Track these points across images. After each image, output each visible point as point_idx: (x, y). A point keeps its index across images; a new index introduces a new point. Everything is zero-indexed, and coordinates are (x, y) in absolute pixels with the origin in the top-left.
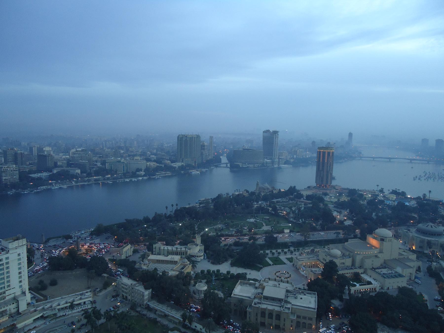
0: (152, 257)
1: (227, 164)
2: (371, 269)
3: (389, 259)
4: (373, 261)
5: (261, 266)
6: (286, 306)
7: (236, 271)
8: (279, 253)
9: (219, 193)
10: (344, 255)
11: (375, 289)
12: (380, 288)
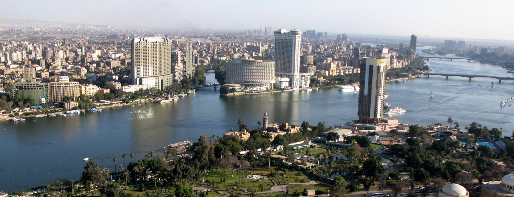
1: (215, 86)
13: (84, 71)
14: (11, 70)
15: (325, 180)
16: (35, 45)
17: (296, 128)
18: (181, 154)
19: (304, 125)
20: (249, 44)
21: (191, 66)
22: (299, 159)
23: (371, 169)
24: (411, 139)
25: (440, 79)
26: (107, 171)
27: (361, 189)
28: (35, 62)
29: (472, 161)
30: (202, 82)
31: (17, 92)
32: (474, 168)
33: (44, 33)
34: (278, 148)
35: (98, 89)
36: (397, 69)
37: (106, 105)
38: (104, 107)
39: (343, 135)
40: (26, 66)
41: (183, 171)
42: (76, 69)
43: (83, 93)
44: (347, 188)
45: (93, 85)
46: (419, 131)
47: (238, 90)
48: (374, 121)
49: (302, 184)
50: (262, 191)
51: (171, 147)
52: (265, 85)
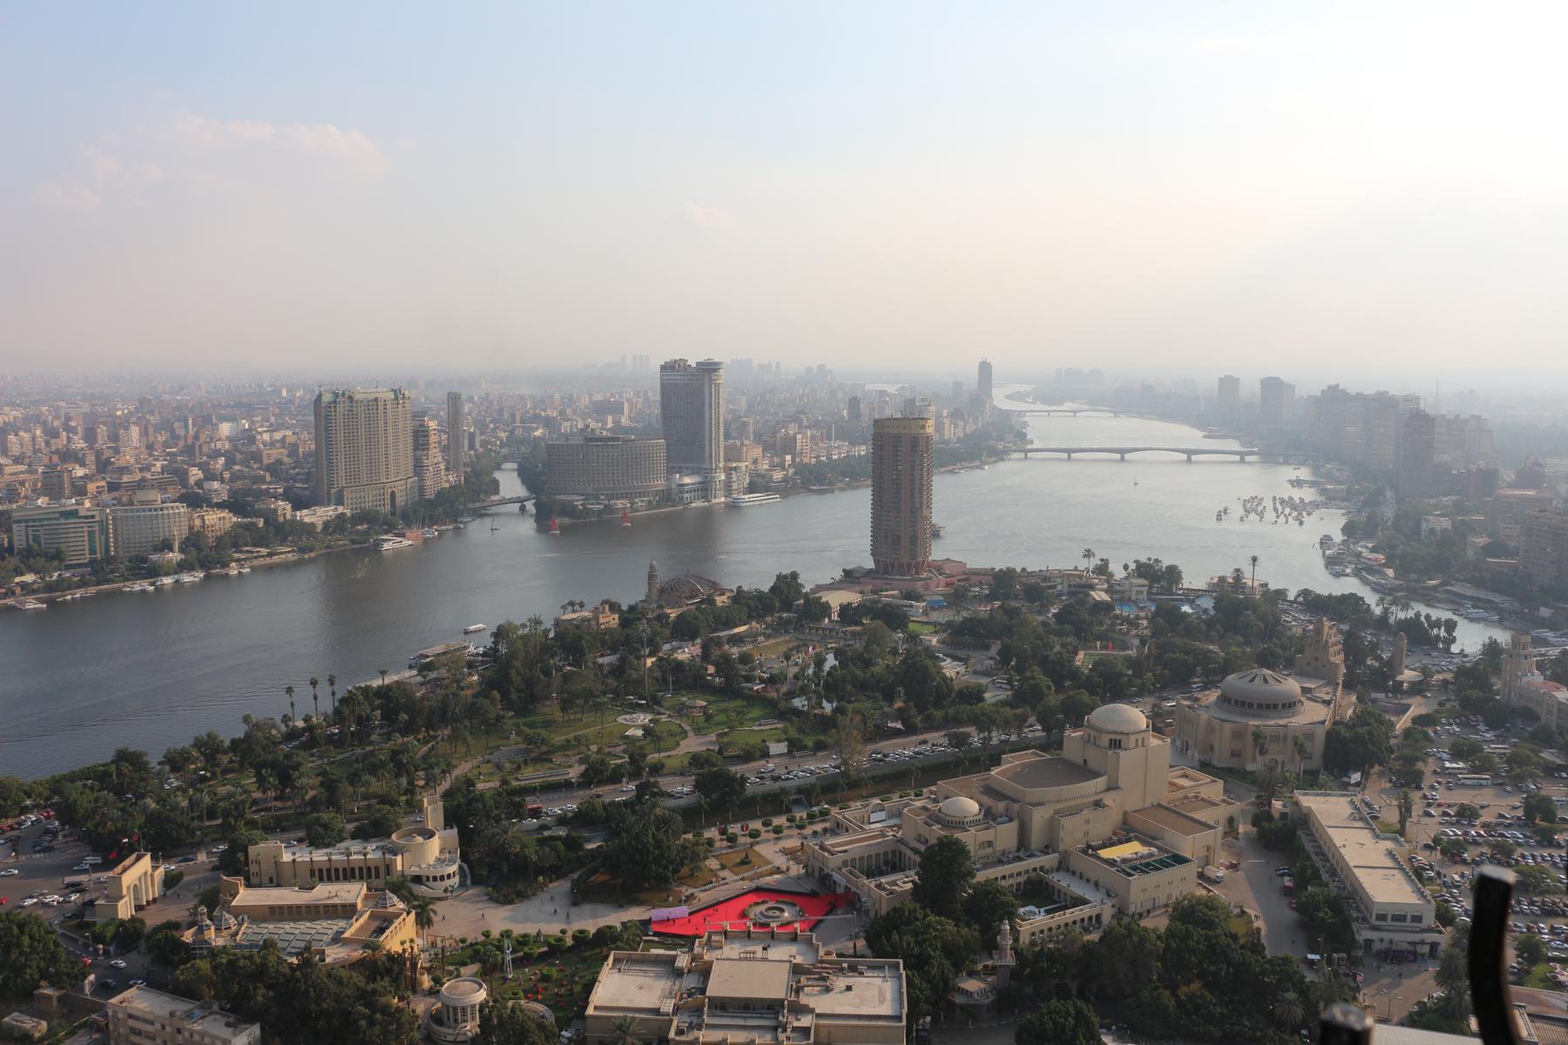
0: (245, 897)
2: (1084, 851)
3: (1139, 806)
4: (1087, 822)
6: (796, 1024)
7: (591, 921)
8: (755, 834)
9: (502, 622)
10: (989, 816)
12: (1114, 911)
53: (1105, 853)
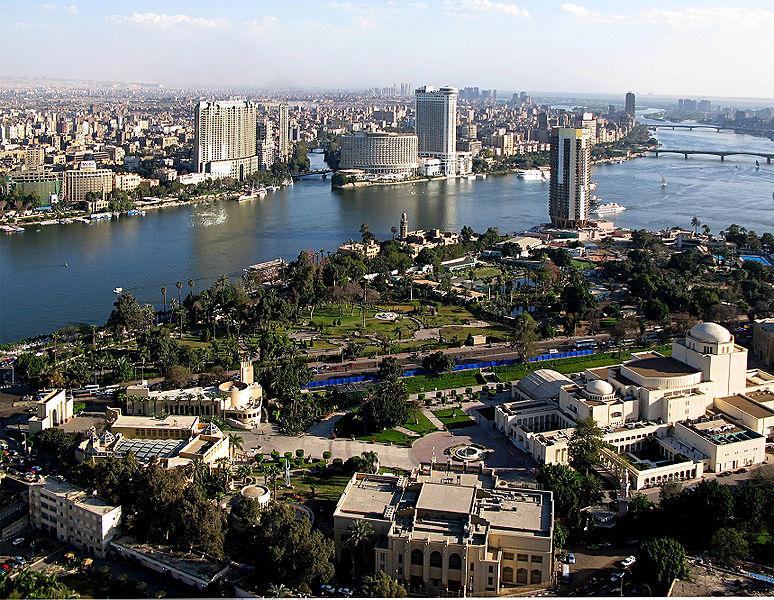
0: (122, 421)
4: (687, 403)
5: (413, 434)
11: (694, 471)
13: (120, 153)
14: (7, 153)
15: (500, 319)
16: (46, 115)
17: (453, 236)
18: (271, 280)
19: (466, 233)
20: (376, 109)
21: (287, 144)
22: (460, 287)
23: (574, 299)
24: (636, 252)
25: (675, 158)
26: (150, 309)
27: (560, 334)
28: (45, 139)
29: (735, 286)
30: (304, 167)
31: (13, 186)
32: (739, 298)
33: (62, 97)
34: (425, 269)
35: (141, 180)
36: (607, 144)
37: (153, 204)
38: (149, 208)
39: (528, 248)
40: (31, 146)
41: (273, 308)
42: (107, 150)
43: (118, 186)
44: (536, 332)
45: (134, 173)
46: (647, 239)
47: (360, 179)
48: (576, 224)
49: (465, 326)
50: (400, 339)
51: (254, 269)
52: (403, 170)
53: (699, 426)
